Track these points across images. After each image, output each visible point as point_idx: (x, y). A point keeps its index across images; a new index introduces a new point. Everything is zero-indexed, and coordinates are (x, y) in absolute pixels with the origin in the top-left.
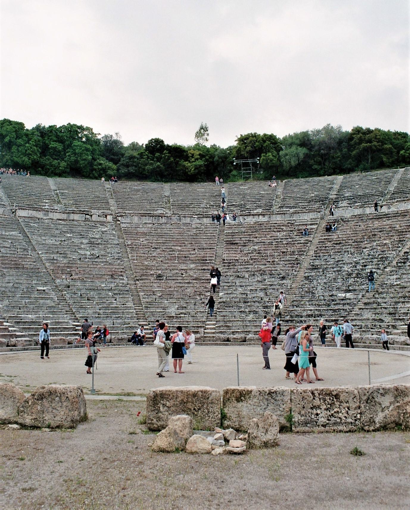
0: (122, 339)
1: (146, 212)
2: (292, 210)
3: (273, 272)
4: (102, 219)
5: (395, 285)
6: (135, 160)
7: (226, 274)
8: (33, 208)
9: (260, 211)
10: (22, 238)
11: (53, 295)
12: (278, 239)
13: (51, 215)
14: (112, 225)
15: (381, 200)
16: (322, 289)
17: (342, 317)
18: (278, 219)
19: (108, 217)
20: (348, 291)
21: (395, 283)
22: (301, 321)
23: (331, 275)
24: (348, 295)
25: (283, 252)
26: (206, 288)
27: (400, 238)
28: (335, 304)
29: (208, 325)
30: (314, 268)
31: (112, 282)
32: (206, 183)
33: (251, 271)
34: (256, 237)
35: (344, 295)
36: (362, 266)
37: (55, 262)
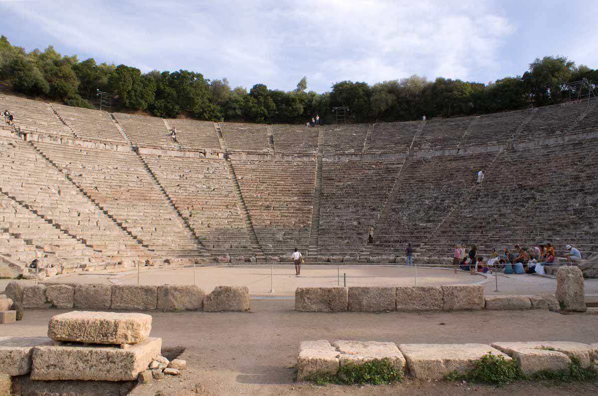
0: (239, 260)
3: (365, 204)
5: (468, 217)
7: (324, 205)
8: (153, 146)
9: (352, 151)
10: (145, 173)
12: (369, 176)
13: (169, 153)
14: (224, 162)
15: (458, 144)
16: (406, 220)
17: (423, 242)
19: (220, 154)
20: (430, 221)
21: (468, 216)
22: (389, 246)
23: (414, 207)
24: (429, 225)
25: (373, 188)
27: (474, 178)
28: (417, 232)
29: (311, 248)
30: (401, 201)
33: (346, 204)
35: (425, 225)
36: (441, 200)
37: (177, 194)
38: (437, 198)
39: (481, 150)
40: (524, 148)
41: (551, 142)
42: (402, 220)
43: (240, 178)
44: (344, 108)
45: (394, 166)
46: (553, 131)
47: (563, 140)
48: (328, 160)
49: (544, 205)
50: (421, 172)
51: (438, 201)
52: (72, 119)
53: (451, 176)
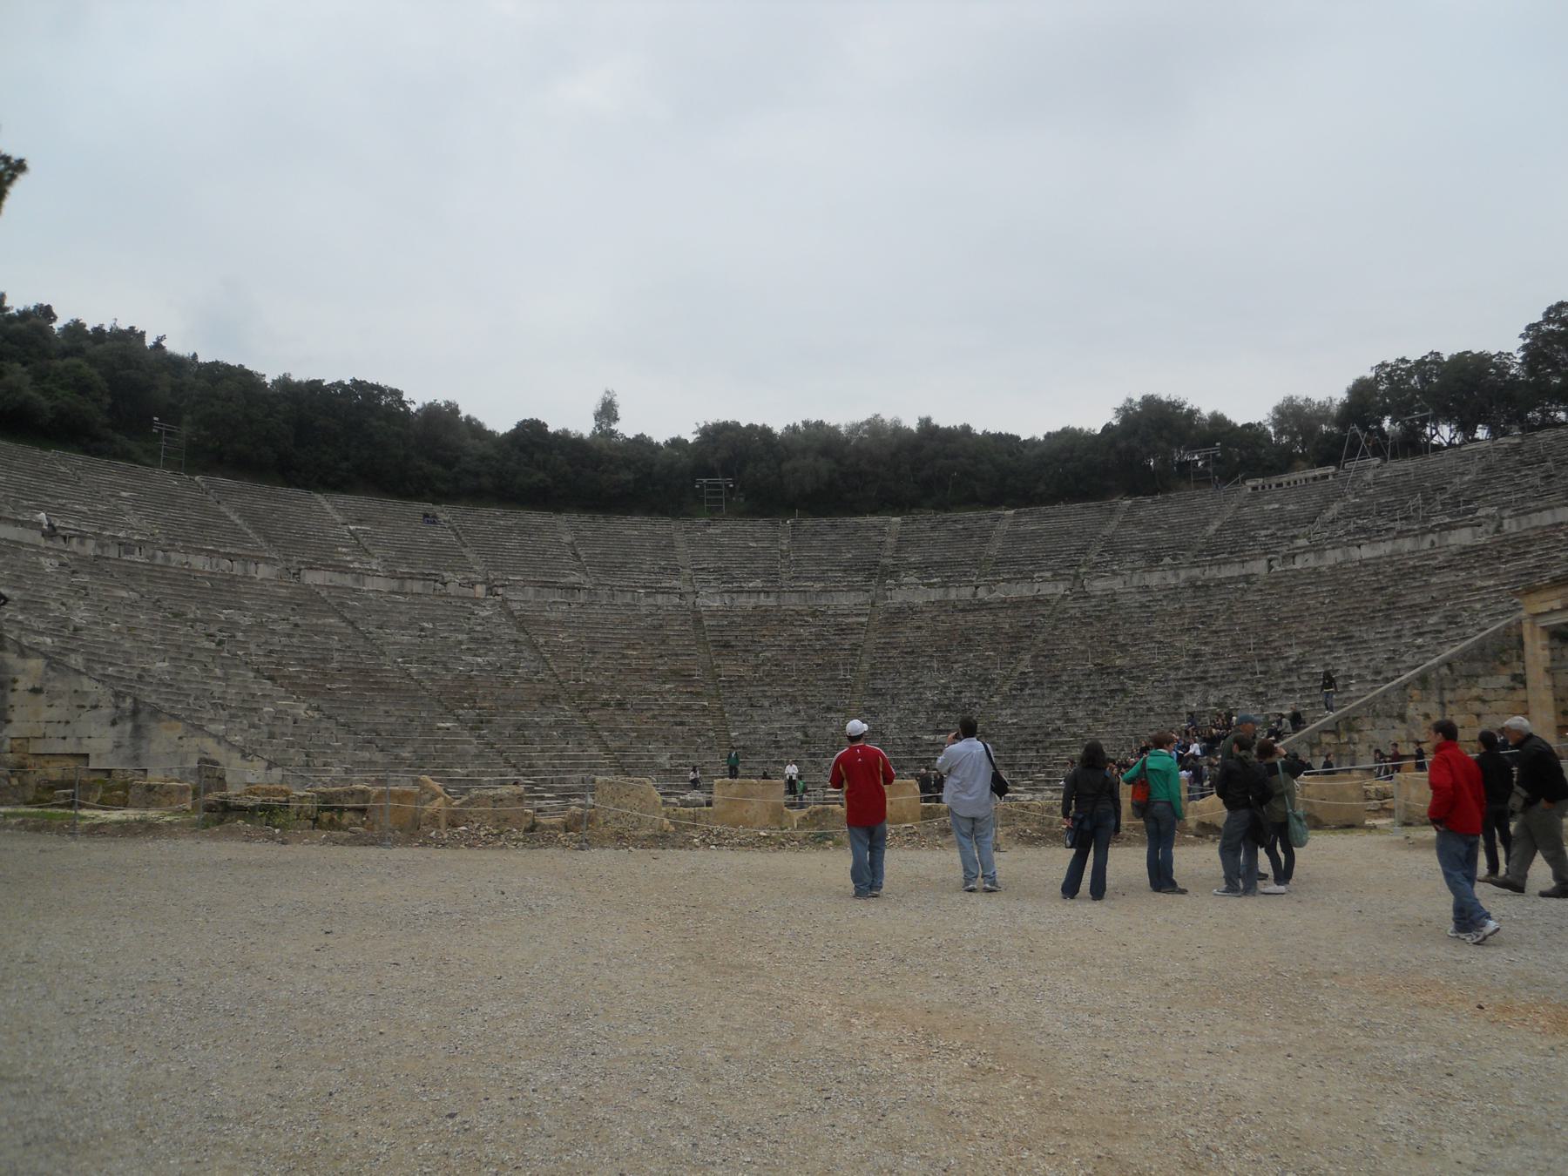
1: (544, 579)
2: (818, 586)
4: (466, 591)
6: (493, 463)
9: (757, 583)
11: (466, 735)
13: (371, 584)
18: (792, 601)
20: (940, 732)
21: (1010, 722)
25: (818, 665)
26: (704, 723)
28: (920, 752)
30: (877, 693)
31: (547, 714)
32: (636, 519)
34: (764, 636)
38: (946, 687)
39: (1022, 590)
40: (1103, 590)
41: (1154, 579)
42: (887, 728)
43: (542, 641)
44: (720, 480)
45: (850, 620)
46: (1159, 559)
47: (1177, 576)
48: (711, 604)
49: (1141, 703)
50: (906, 634)
51: (950, 694)
52: (124, 494)
53: (967, 642)
